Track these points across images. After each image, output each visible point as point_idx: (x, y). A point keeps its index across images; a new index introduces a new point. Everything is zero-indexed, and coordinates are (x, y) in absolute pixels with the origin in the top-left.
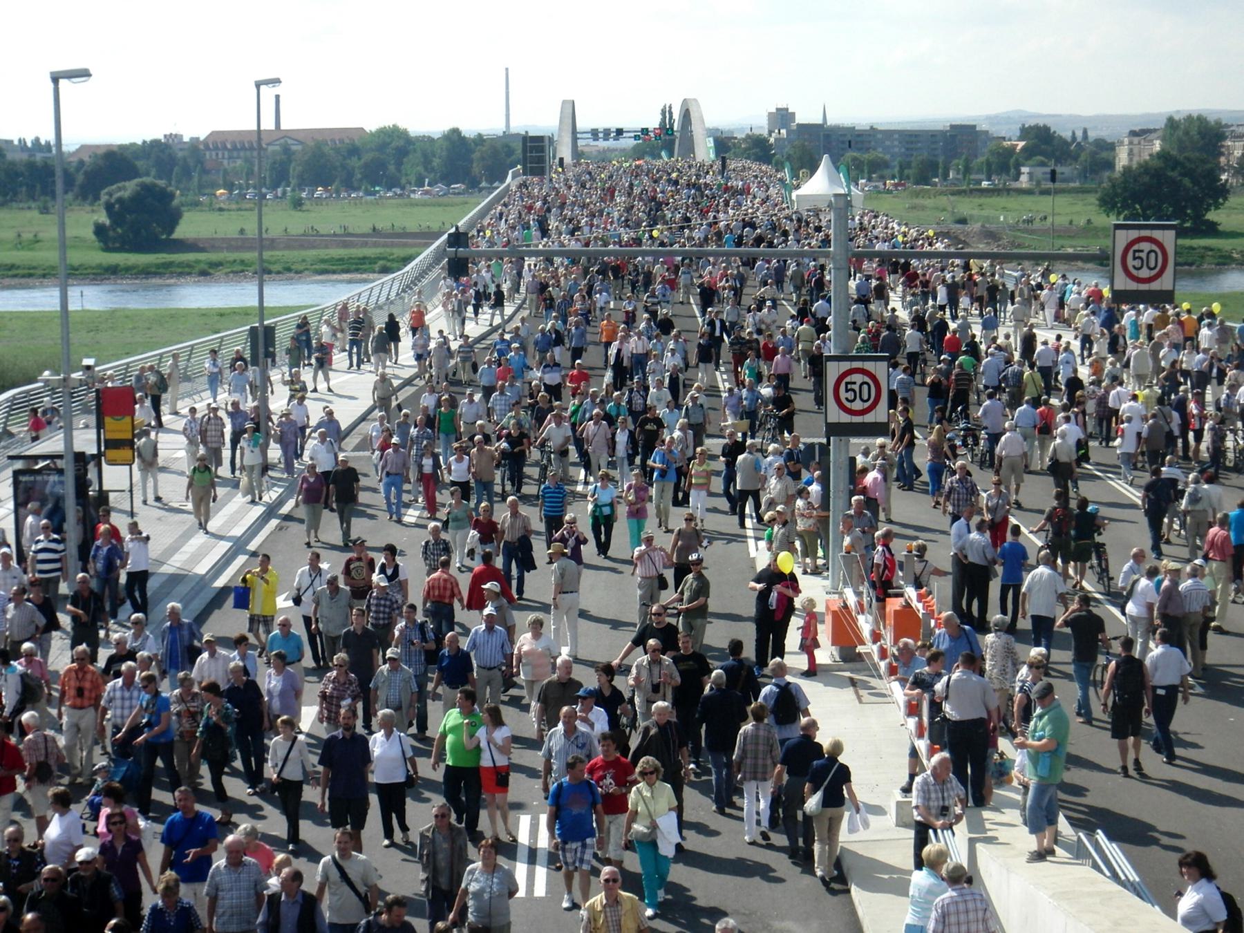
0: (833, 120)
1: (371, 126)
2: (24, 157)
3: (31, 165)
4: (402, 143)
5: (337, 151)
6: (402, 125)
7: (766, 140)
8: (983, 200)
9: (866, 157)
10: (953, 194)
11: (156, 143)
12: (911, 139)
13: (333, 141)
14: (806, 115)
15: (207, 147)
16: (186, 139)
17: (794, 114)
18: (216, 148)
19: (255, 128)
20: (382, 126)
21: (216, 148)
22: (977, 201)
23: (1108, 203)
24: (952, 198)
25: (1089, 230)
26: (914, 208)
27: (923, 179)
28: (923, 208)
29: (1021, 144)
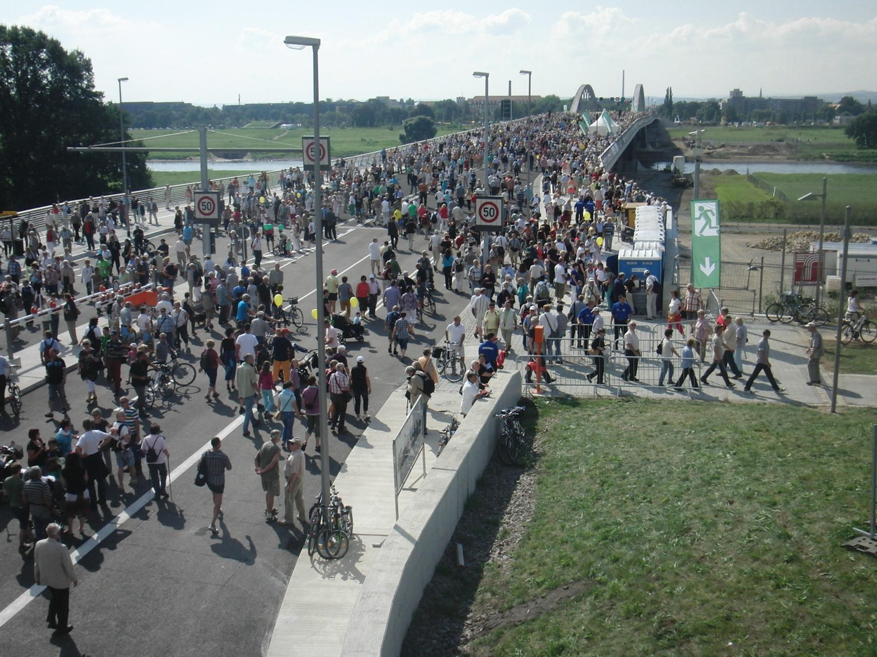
0: (766, 95)
1: (543, 95)
2: (401, 107)
3: (393, 110)
4: (553, 102)
5: (525, 105)
6: (557, 95)
7: (717, 104)
8: (803, 131)
9: (765, 111)
10: (789, 128)
11: (450, 102)
12: (786, 104)
13: (523, 101)
14: (749, 92)
15: (473, 102)
16: (466, 99)
17: (742, 92)
18: (477, 104)
19: (484, 95)
20: (551, 94)
21: (477, 104)
22: (799, 131)
23: (850, 132)
24: (788, 130)
25: (840, 146)
26: (767, 134)
27: (784, 120)
28: (772, 134)
29: (839, 106)
